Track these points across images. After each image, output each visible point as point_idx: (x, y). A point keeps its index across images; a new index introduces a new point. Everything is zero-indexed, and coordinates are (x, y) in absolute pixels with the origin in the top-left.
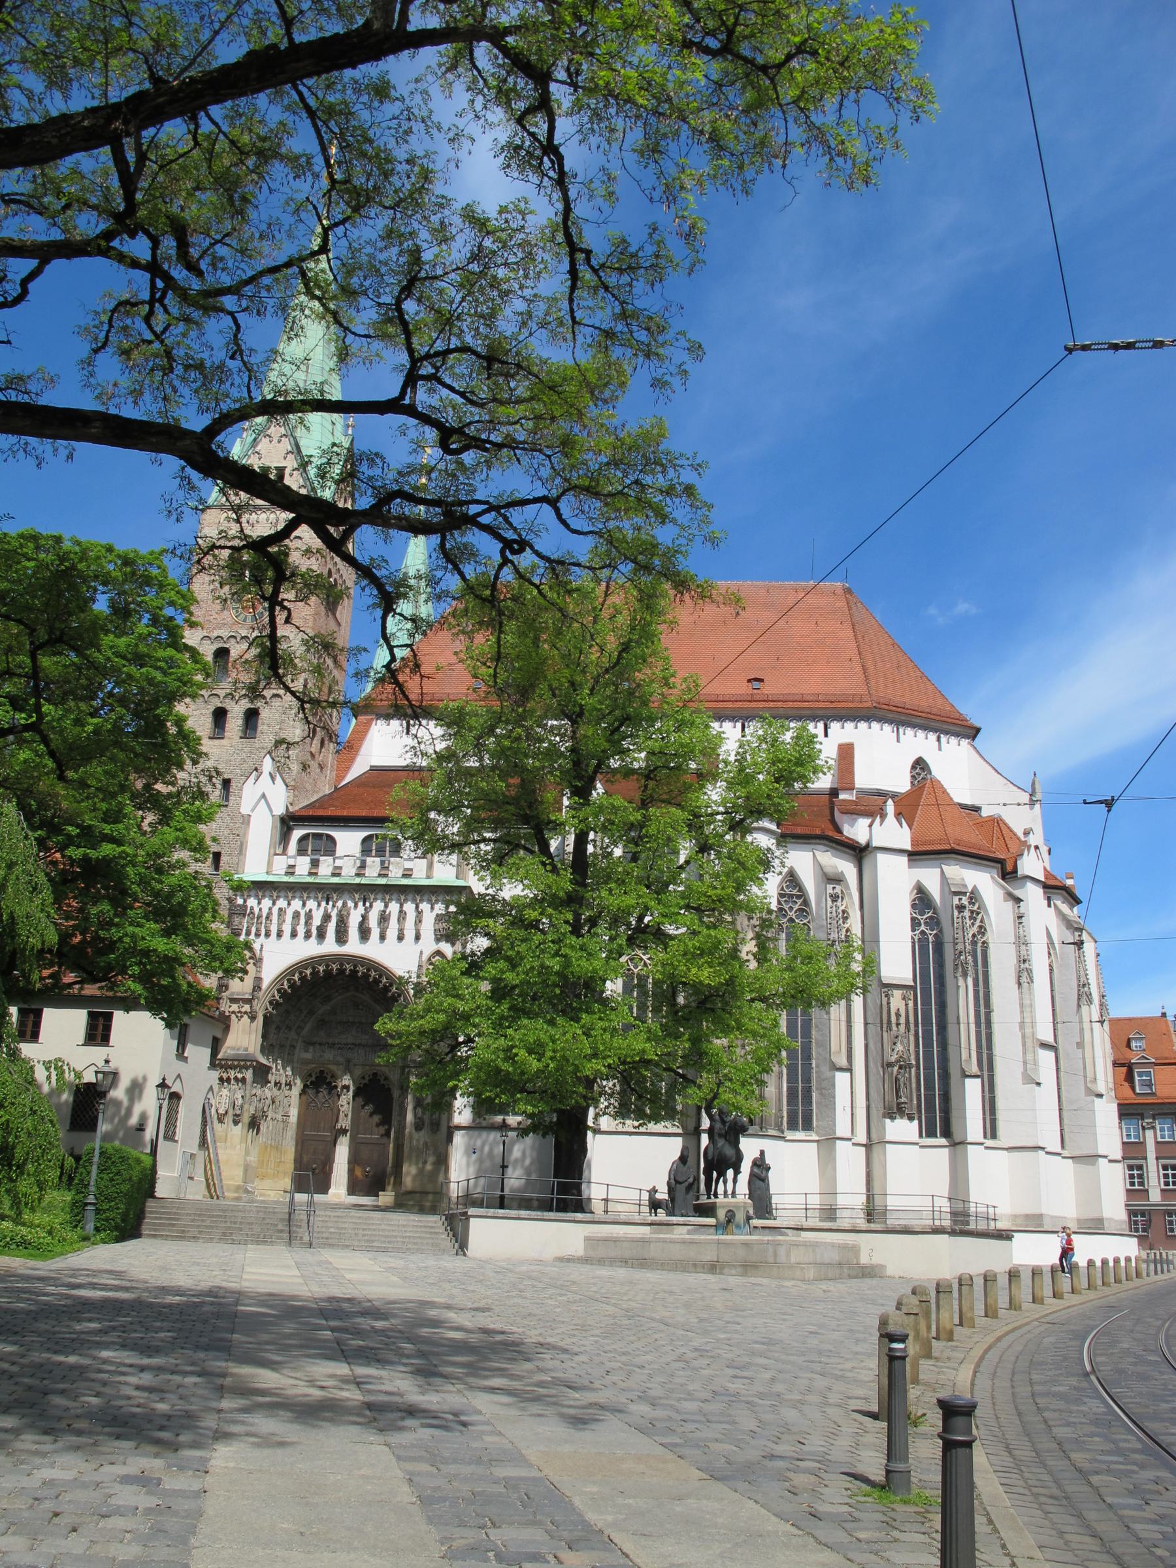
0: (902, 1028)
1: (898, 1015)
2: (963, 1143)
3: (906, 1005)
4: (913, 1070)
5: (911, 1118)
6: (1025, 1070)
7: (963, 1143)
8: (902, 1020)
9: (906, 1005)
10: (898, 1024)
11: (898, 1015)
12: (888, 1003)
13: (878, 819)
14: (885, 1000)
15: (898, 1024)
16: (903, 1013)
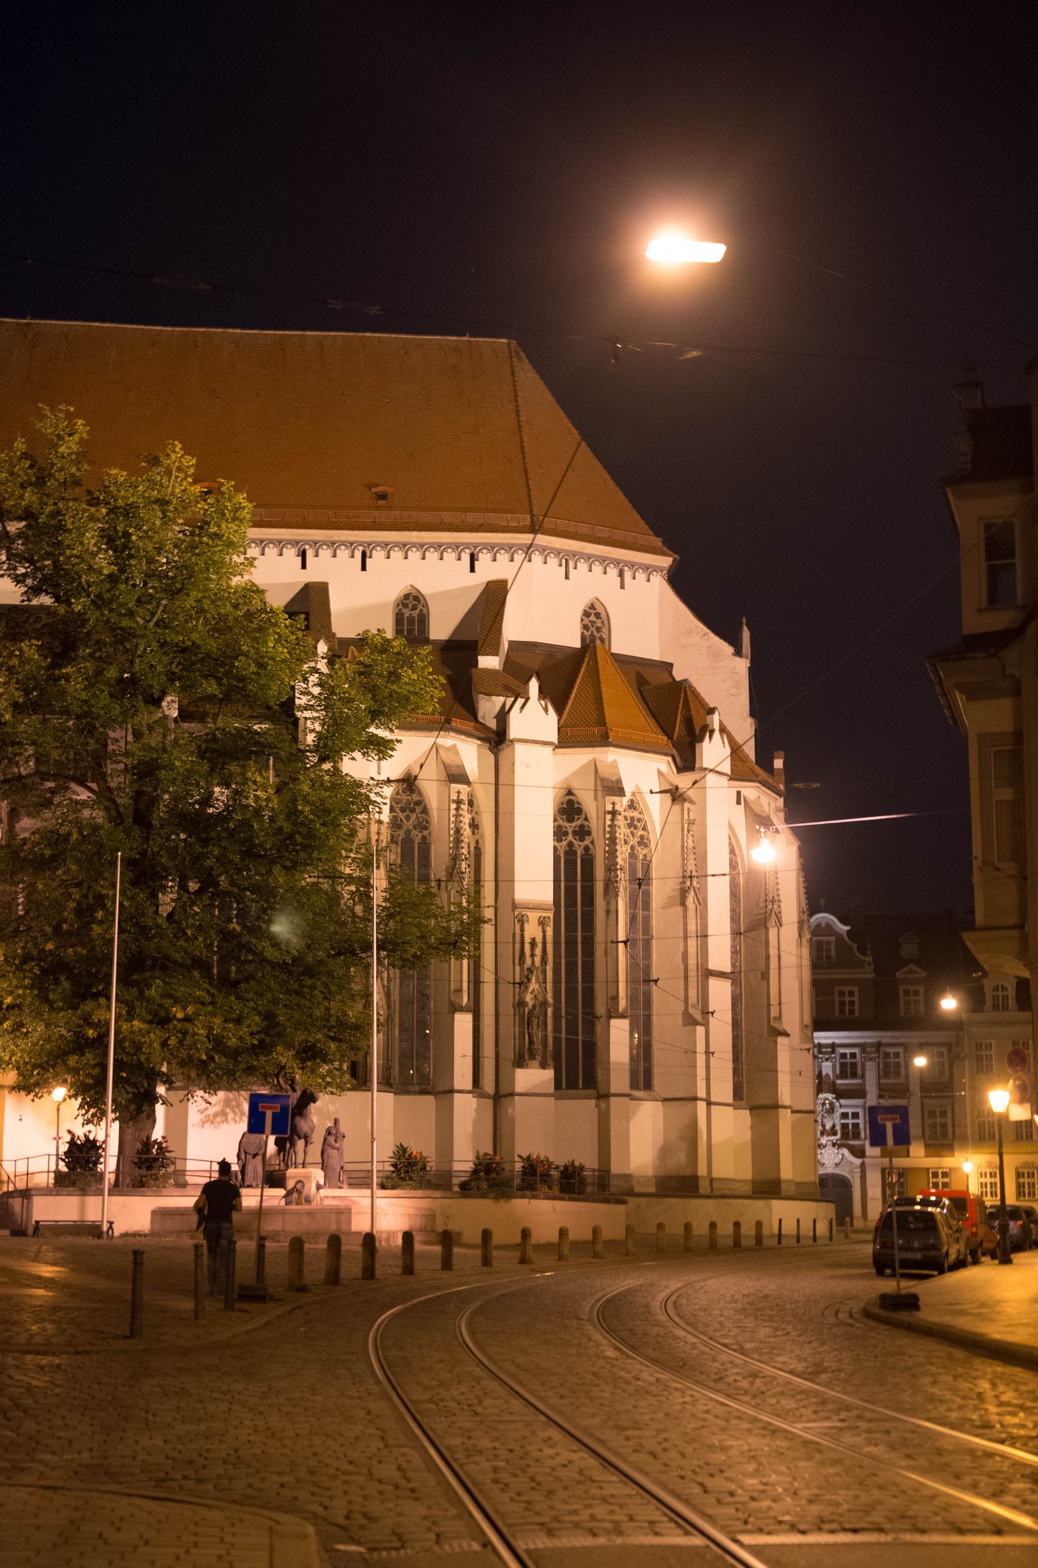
0: (538, 960)
1: (533, 943)
2: (607, 1096)
3: (544, 932)
4: (550, 1011)
5: (543, 1066)
6: (686, 1008)
7: (607, 1096)
8: (538, 951)
9: (544, 932)
10: (533, 955)
11: (533, 943)
12: (522, 930)
13: (520, 701)
14: (518, 926)
15: (533, 955)
16: (539, 940)
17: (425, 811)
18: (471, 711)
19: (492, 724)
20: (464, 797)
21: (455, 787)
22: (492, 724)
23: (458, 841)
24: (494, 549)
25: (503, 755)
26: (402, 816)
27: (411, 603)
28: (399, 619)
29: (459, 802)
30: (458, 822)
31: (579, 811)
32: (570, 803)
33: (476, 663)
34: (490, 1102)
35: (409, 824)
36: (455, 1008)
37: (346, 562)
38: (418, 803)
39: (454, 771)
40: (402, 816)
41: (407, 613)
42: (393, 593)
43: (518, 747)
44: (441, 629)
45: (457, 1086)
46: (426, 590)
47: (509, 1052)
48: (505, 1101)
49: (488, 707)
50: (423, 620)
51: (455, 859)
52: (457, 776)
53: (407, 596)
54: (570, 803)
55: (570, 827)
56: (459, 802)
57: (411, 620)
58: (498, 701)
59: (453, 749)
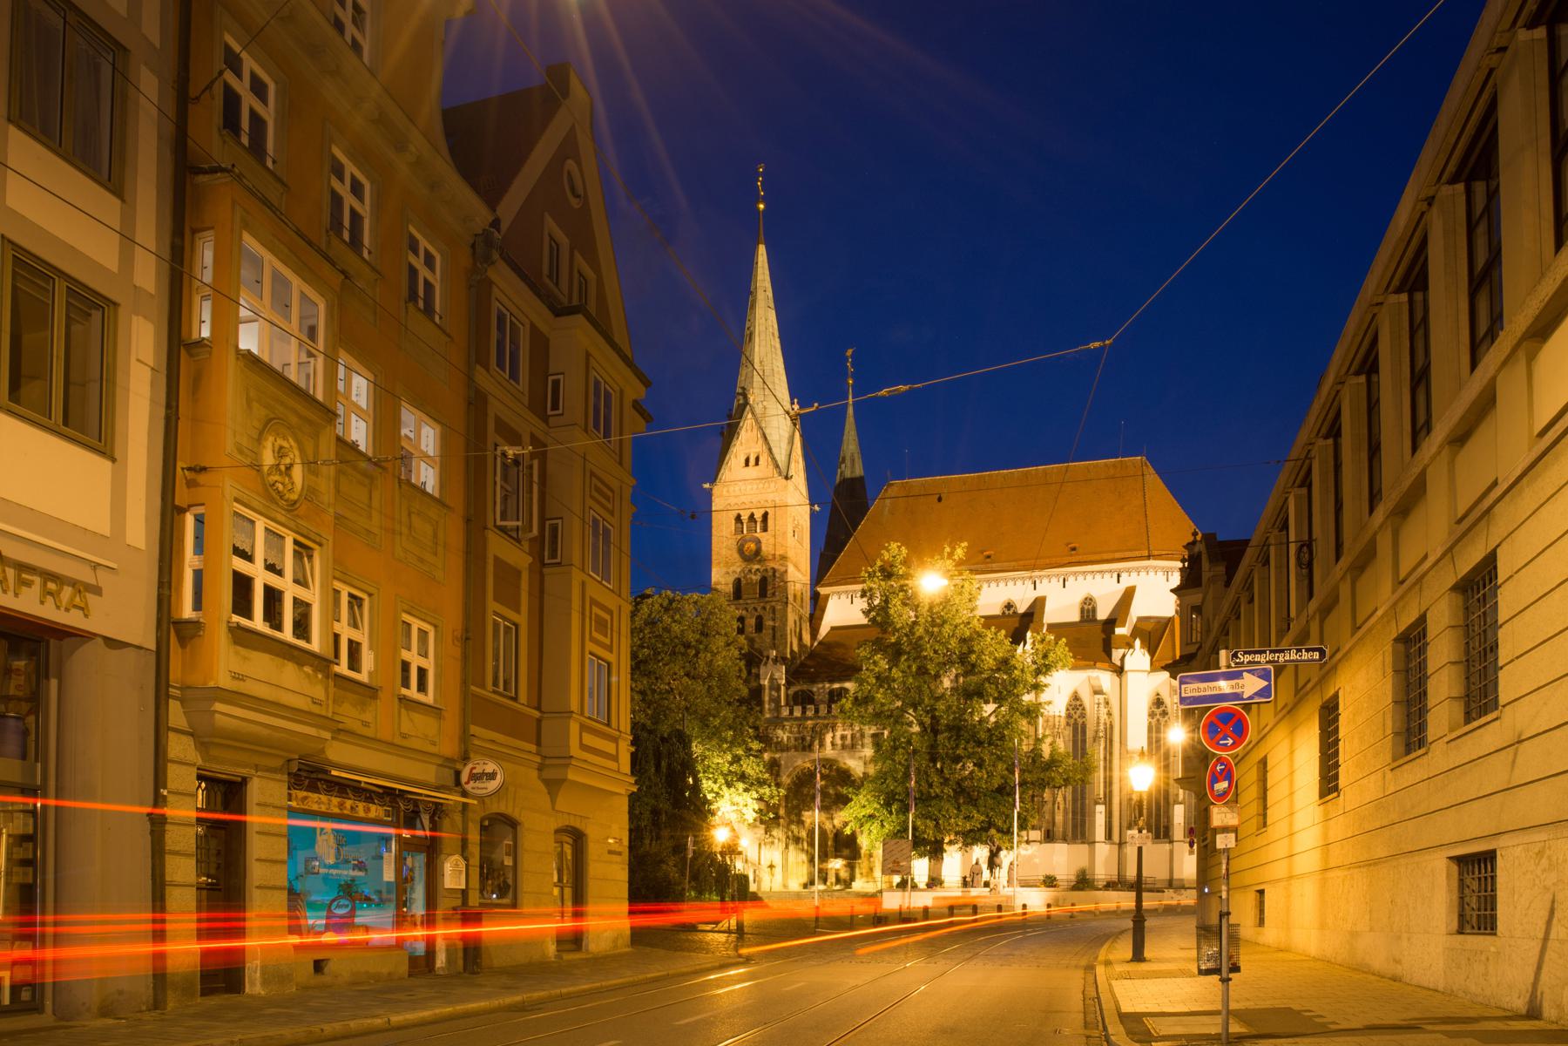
17: (1084, 709)
18: (1109, 655)
19: (1118, 663)
20: (1102, 701)
21: (1097, 696)
22: (1118, 663)
23: (1098, 723)
24: (1129, 571)
25: (1123, 679)
26: (1072, 712)
27: (1088, 602)
28: (1082, 610)
29: (1099, 704)
30: (1098, 713)
31: (1162, 703)
32: (1158, 699)
33: (1114, 632)
34: (1117, 847)
35: (1076, 716)
36: (1097, 803)
37: (1056, 584)
38: (1080, 705)
39: (1097, 689)
40: (1072, 712)
41: (1086, 607)
42: (1079, 598)
43: (1129, 674)
44: (1103, 614)
45: (1097, 839)
46: (1095, 594)
47: (1125, 824)
48: (1123, 846)
49: (1117, 654)
50: (1094, 610)
51: (1097, 732)
52: (1098, 692)
53: (1086, 599)
54: (1158, 699)
55: (1158, 711)
56: (1099, 704)
57: (1088, 610)
58: (1122, 651)
59: (1097, 678)
